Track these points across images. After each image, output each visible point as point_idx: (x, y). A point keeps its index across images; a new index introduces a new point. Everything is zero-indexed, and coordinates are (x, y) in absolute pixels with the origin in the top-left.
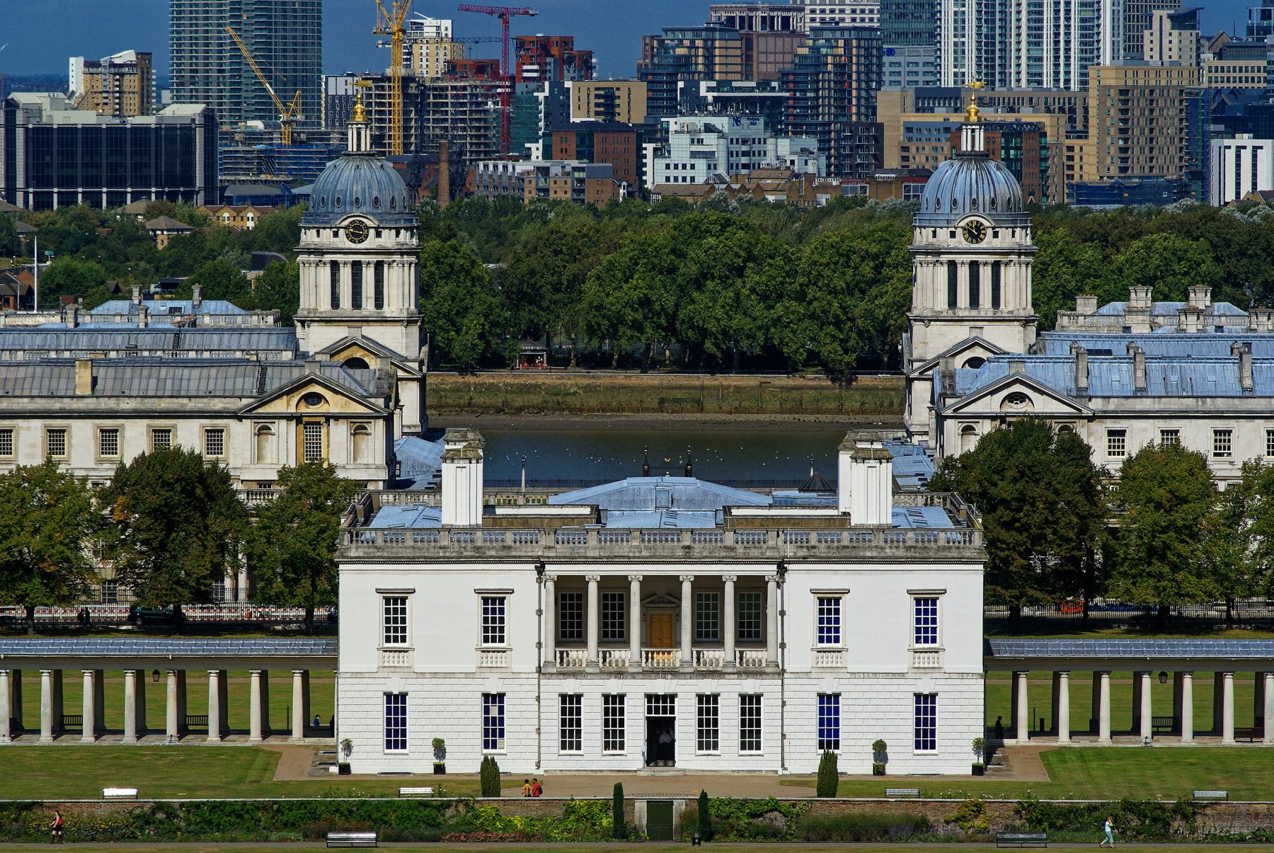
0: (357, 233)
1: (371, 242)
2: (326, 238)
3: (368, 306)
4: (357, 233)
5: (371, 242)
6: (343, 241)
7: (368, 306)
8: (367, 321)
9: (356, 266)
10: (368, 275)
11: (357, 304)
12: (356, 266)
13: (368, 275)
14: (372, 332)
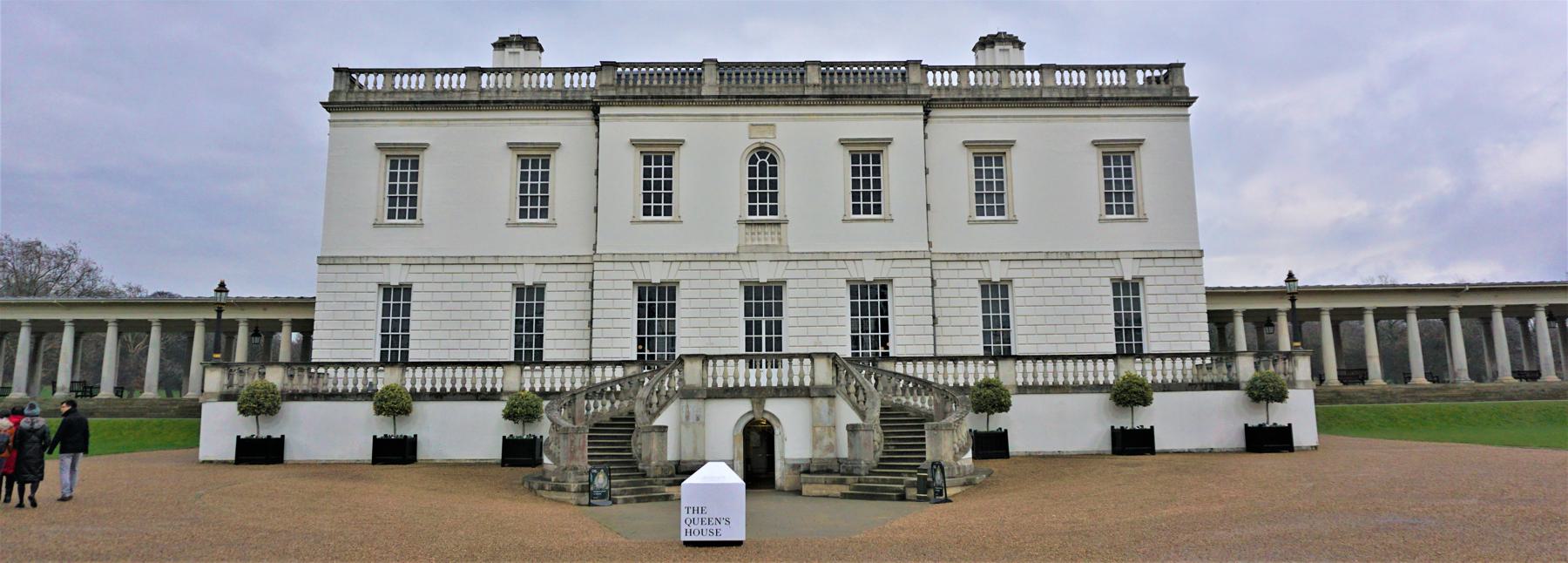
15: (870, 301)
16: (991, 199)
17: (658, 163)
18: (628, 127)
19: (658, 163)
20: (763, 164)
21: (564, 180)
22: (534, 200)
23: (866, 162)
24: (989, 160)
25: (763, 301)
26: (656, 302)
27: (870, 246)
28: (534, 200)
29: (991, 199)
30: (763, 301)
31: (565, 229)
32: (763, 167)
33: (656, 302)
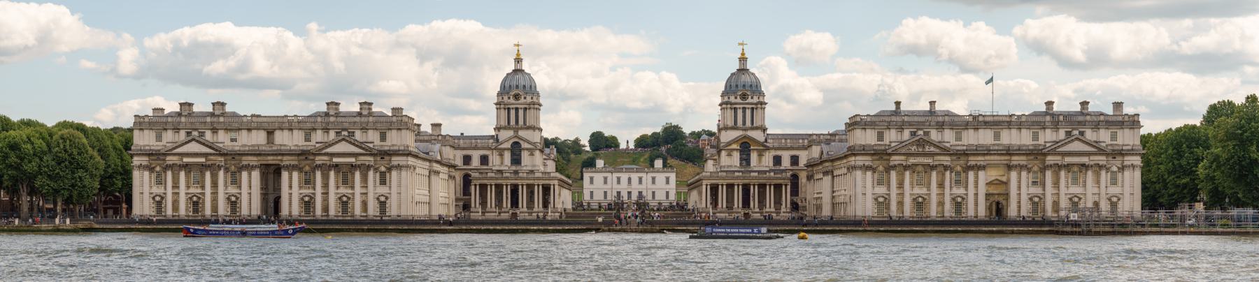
0: (744, 97)
1: (750, 100)
2: (732, 99)
3: (748, 124)
4: (744, 97)
5: (750, 100)
6: (739, 100)
7: (748, 124)
8: (746, 130)
9: (744, 109)
10: (748, 112)
11: (744, 123)
12: (744, 109)
13: (748, 112)
14: (750, 133)
15: (640, 193)
16: (654, 182)
17: (619, 179)
18: (616, 175)
19: (619, 179)
20: (630, 179)
21: (609, 180)
22: (605, 182)
23: (640, 179)
24: (654, 179)
25: (629, 193)
26: (619, 193)
27: (642, 187)
28: (605, 182)
29: (654, 182)
30: (629, 193)
31: (609, 186)
32: (630, 179)
33: (619, 193)
